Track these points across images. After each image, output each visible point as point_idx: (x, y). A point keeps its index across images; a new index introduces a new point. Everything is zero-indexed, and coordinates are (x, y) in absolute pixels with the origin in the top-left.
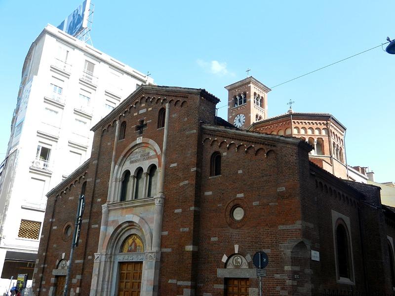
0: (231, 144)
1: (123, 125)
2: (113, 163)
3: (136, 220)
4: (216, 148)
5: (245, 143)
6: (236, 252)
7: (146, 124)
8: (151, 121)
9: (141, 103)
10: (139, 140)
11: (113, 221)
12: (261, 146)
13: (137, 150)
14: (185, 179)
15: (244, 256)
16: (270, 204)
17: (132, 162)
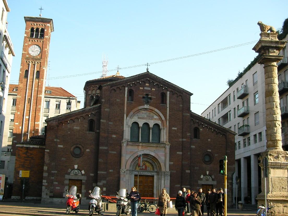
0: (205, 126)
1: (131, 93)
2: (125, 115)
3: (153, 154)
4: (196, 125)
5: (212, 127)
6: (208, 174)
7: (151, 98)
8: (155, 97)
9: (145, 83)
10: (146, 106)
11: (131, 152)
12: (220, 131)
13: (143, 111)
14: (182, 138)
15: (211, 177)
16: (223, 156)
17: (139, 118)
